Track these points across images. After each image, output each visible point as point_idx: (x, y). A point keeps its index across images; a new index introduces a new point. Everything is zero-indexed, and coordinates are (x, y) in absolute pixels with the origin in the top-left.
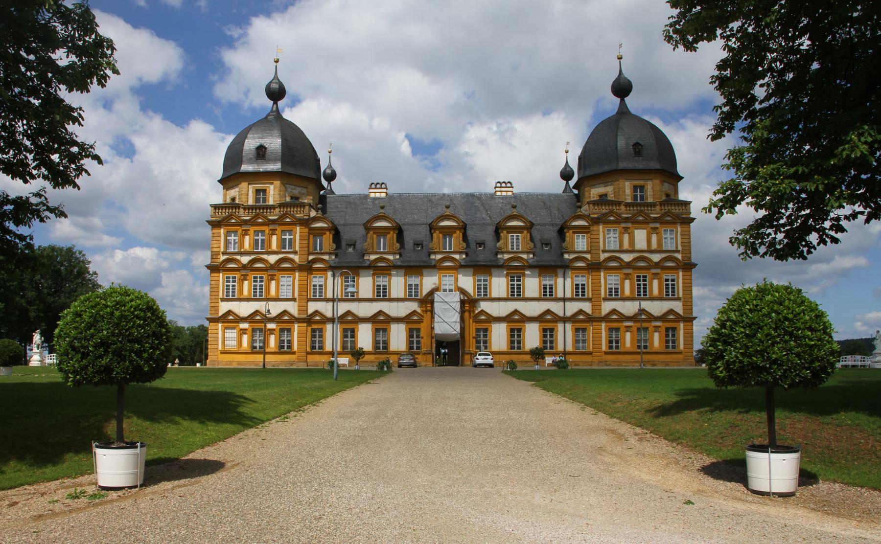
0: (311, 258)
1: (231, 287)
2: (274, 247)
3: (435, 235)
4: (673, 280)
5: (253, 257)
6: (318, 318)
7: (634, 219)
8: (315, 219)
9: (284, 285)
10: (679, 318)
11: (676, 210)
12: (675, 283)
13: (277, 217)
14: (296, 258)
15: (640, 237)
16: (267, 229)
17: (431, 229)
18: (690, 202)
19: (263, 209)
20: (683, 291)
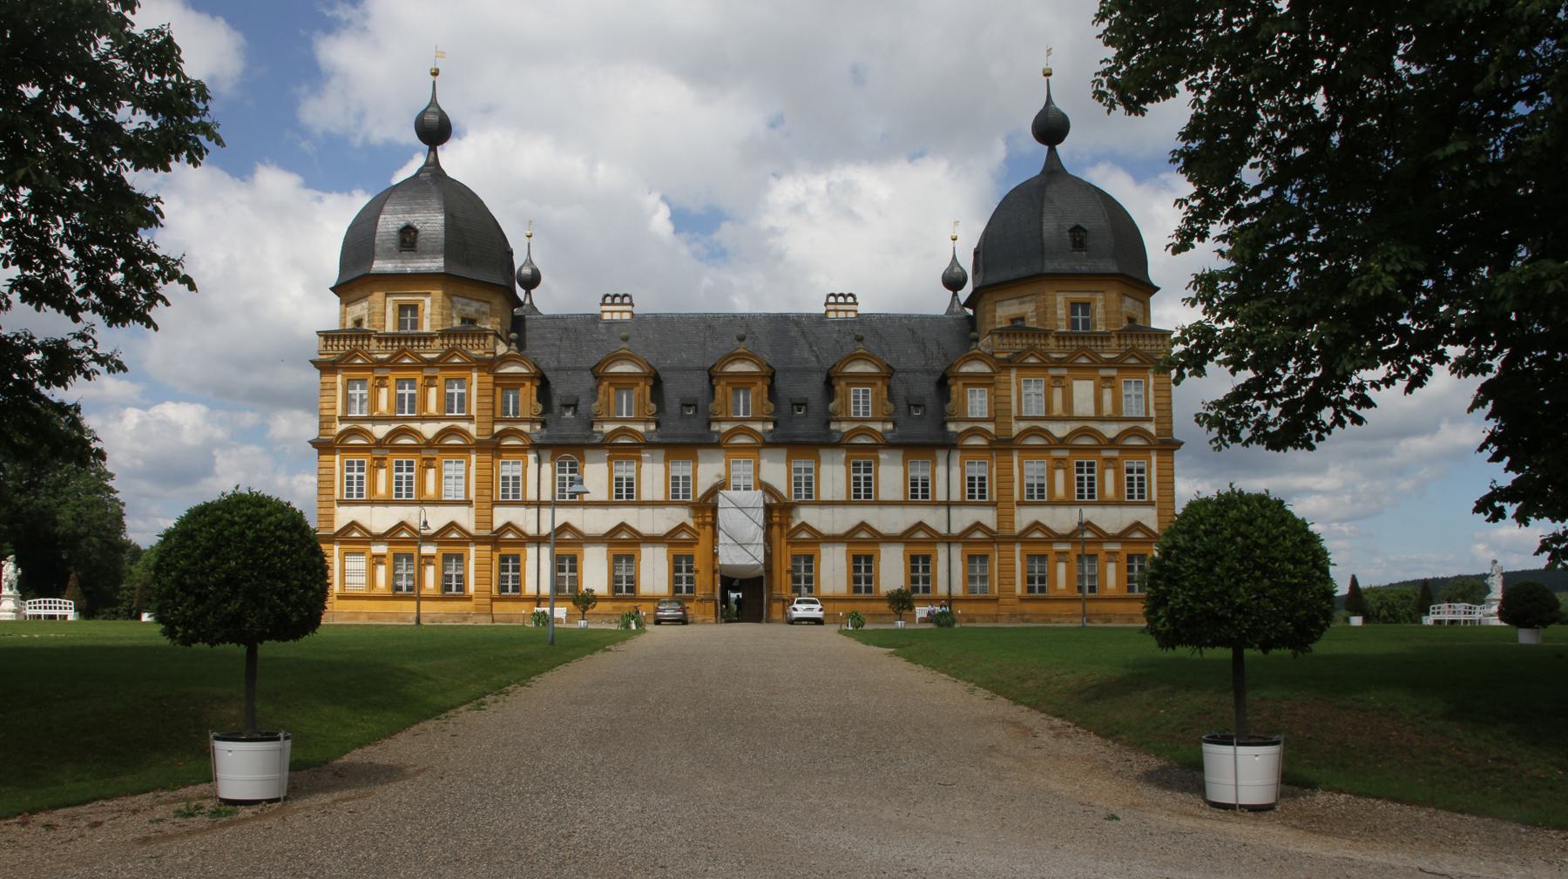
0: (498, 428)
1: (355, 481)
2: (432, 408)
3: (718, 388)
4: (1140, 471)
5: (394, 426)
6: (510, 536)
7: (1072, 363)
8: (505, 359)
9: (451, 477)
11: (1145, 345)
12: (1145, 475)
13: (436, 356)
14: (472, 429)
15: (1083, 393)
16: (419, 377)
17: (711, 378)
19: (413, 340)
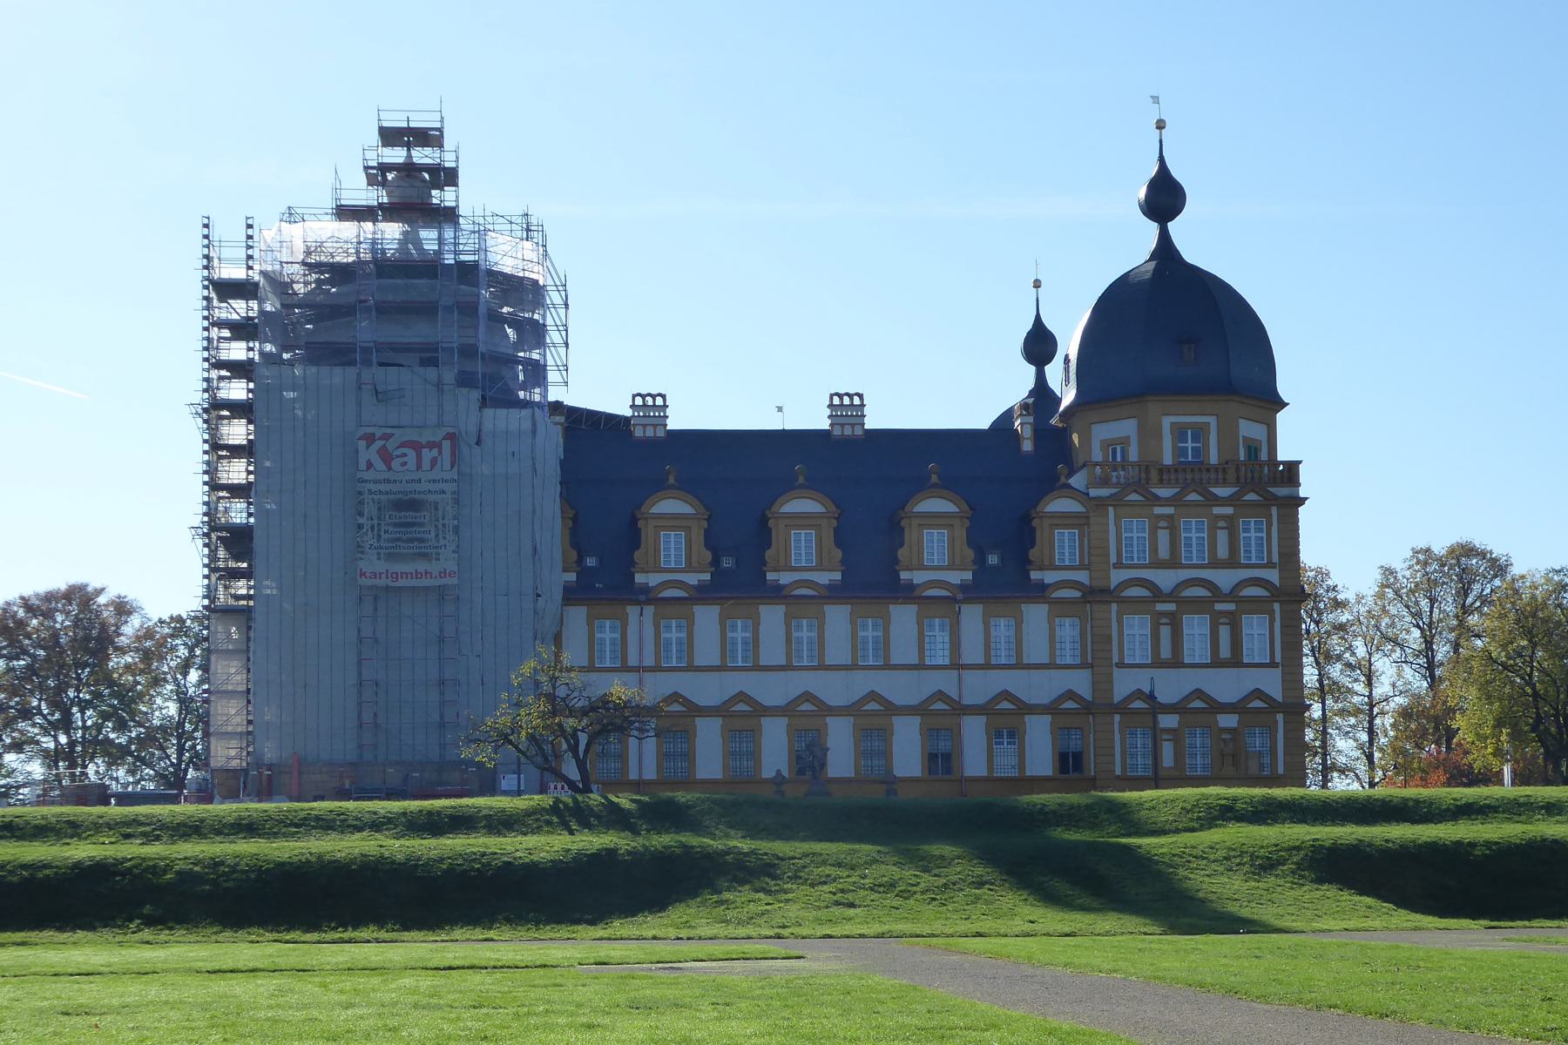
10: (1273, 706)
15: (1193, 532)
18: (1301, 462)
20: (1282, 649)
